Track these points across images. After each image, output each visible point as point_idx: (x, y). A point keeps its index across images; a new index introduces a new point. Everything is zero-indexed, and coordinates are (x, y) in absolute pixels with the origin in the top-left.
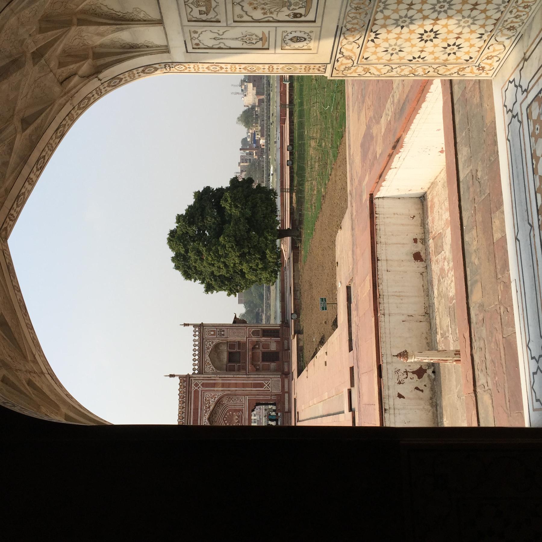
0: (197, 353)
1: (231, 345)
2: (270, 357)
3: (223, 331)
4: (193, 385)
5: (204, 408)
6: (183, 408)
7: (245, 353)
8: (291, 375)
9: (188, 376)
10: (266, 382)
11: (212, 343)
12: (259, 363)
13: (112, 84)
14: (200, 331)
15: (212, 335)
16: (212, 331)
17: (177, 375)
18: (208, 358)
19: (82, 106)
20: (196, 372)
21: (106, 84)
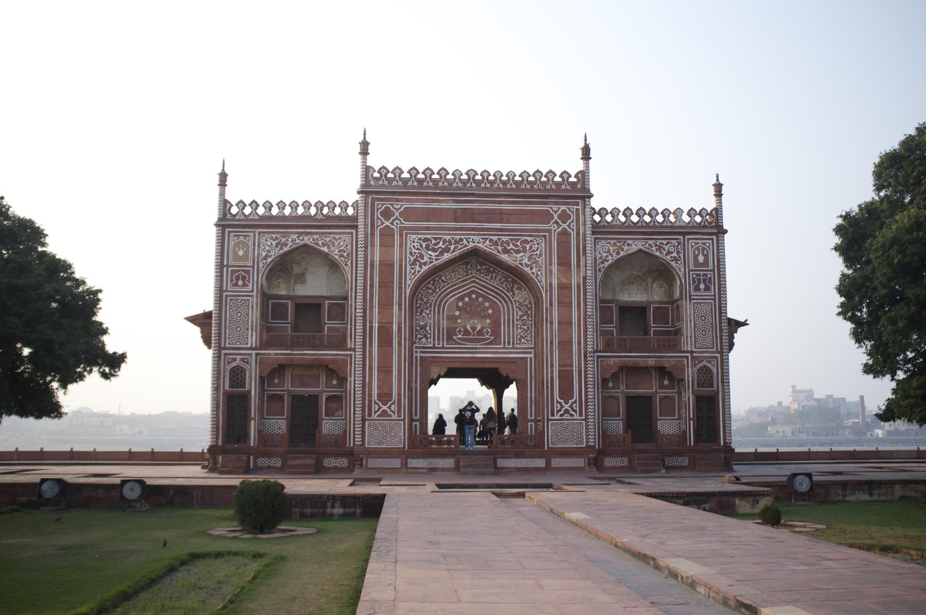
0: (647, 219)
1: (669, 312)
2: (640, 415)
3: (707, 289)
4: (563, 207)
5: (505, 239)
8: (597, 475)
9: (586, 195)
10: (576, 406)
11: (676, 260)
12: (622, 388)
14: (705, 227)
15: (696, 257)
16: (706, 257)
17: (587, 166)
20: (597, 218)
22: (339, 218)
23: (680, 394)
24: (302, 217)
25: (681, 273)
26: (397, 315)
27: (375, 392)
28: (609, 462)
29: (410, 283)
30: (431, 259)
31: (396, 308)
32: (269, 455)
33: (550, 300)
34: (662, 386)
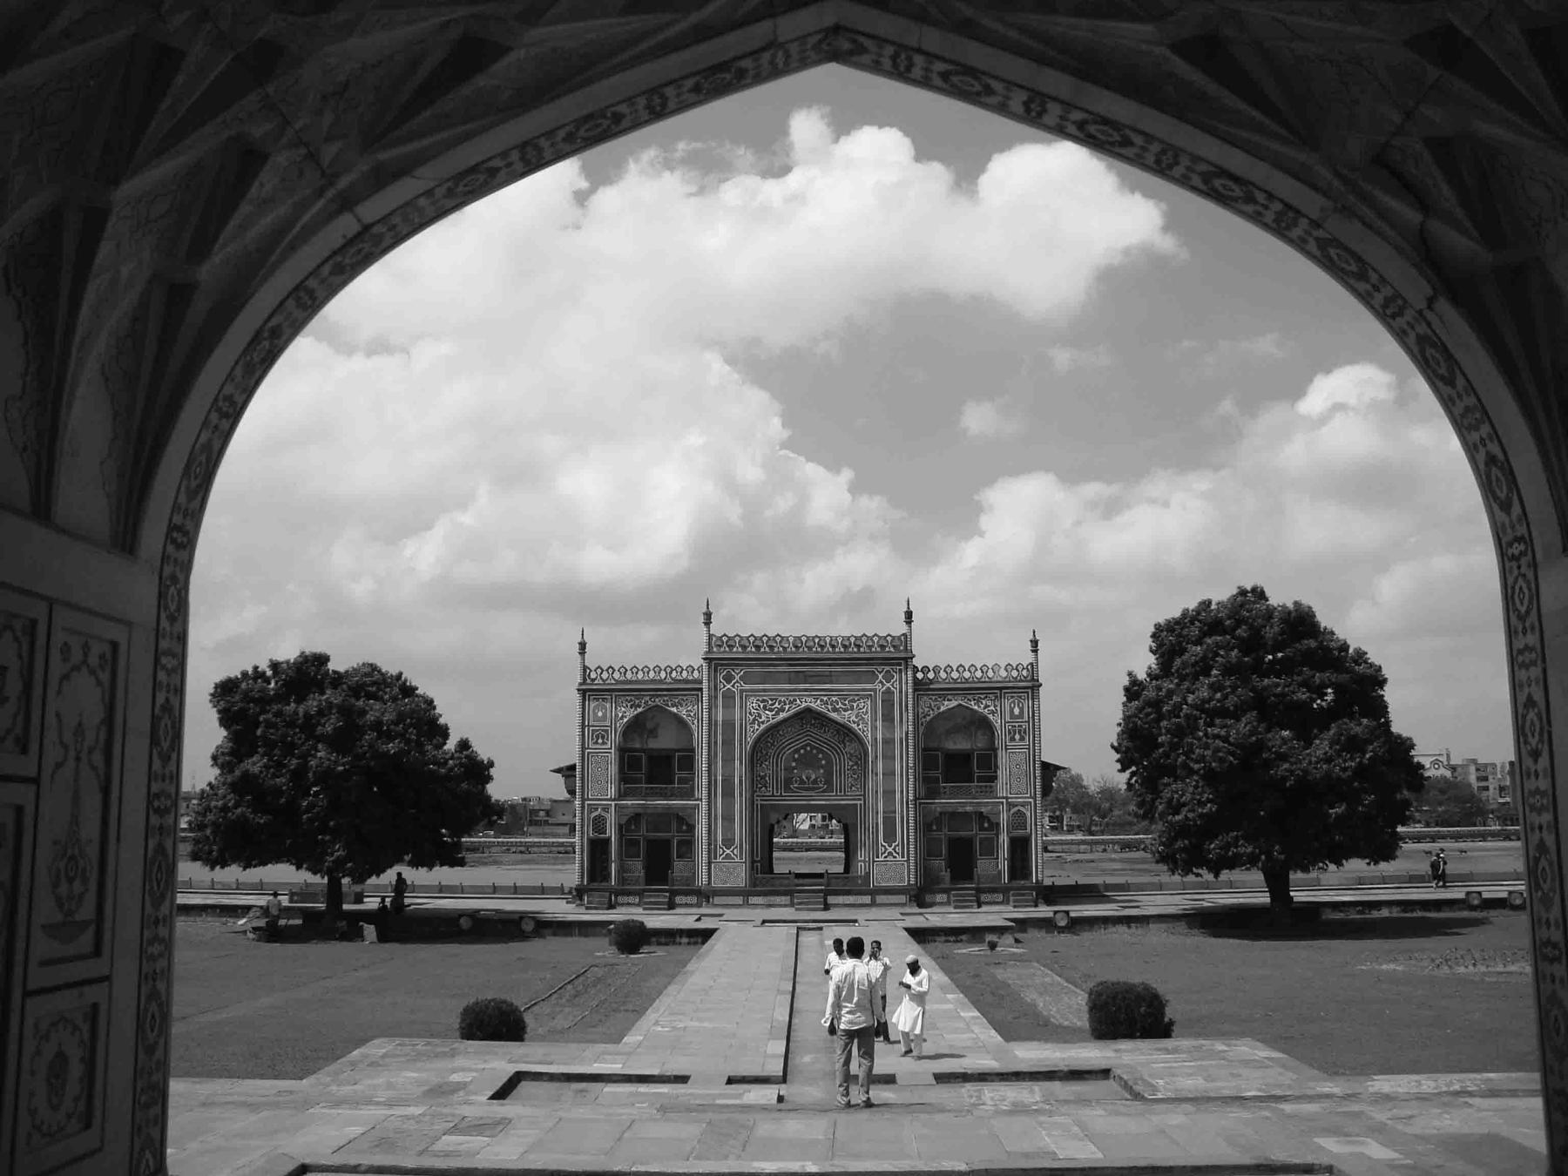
0: (967, 675)
3: (1022, 739)
6: (833, 647)
7: (968, 794)
11: (993, 713)
12: (945, 830)
13: (1430, 351)
16: (1022, 710)
18: (954, 703)
19: (1332, 252)
20: (920, 675)
21: (1422, 329)
22: (686, 681)
23: (997, 835)
24: (653, 681)
25: (998, 726)
26: (739, 770)
27: (720, 838)
28: (928, 898)
29: (750, 741)
30: (768, 718)
31: (737, 763)
32: (629, 893)
33: (875, 752)
34: (982, 829)
